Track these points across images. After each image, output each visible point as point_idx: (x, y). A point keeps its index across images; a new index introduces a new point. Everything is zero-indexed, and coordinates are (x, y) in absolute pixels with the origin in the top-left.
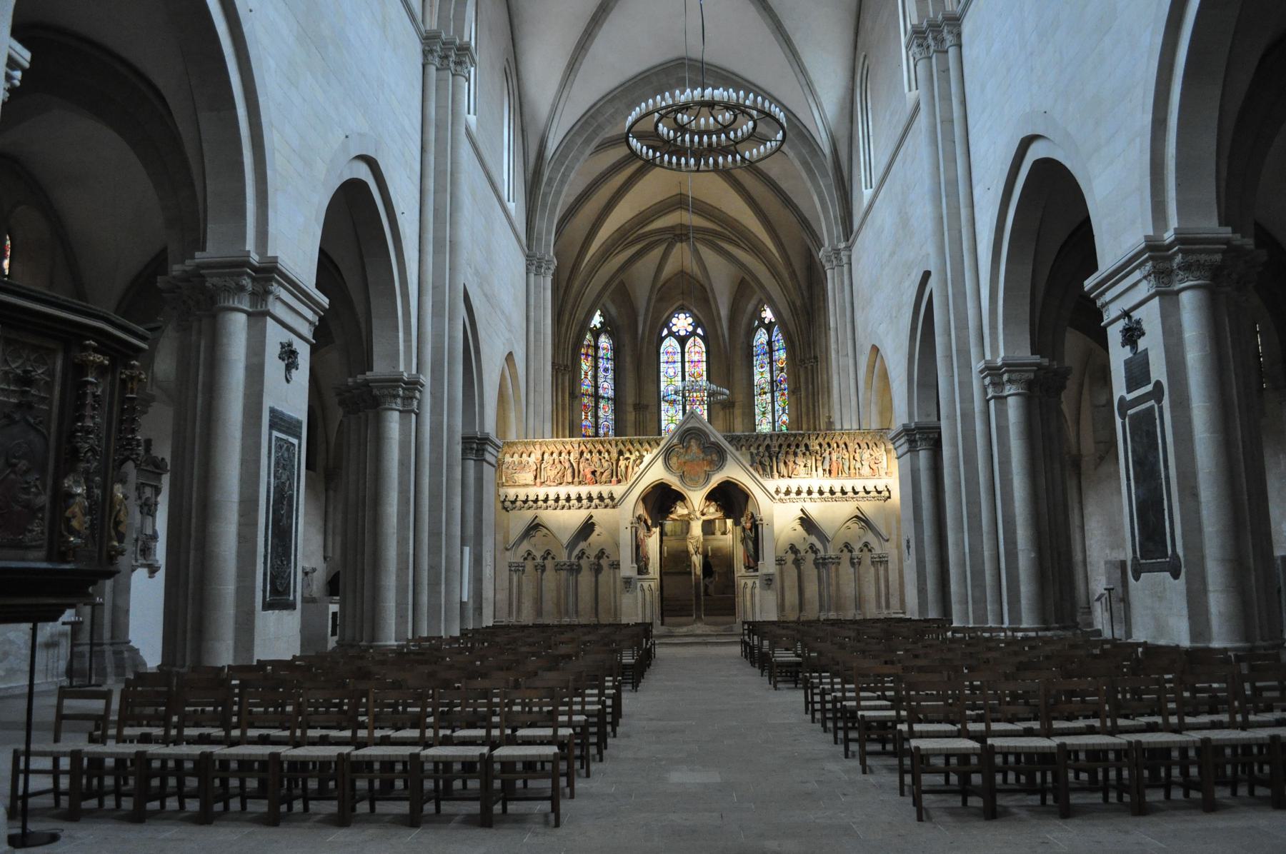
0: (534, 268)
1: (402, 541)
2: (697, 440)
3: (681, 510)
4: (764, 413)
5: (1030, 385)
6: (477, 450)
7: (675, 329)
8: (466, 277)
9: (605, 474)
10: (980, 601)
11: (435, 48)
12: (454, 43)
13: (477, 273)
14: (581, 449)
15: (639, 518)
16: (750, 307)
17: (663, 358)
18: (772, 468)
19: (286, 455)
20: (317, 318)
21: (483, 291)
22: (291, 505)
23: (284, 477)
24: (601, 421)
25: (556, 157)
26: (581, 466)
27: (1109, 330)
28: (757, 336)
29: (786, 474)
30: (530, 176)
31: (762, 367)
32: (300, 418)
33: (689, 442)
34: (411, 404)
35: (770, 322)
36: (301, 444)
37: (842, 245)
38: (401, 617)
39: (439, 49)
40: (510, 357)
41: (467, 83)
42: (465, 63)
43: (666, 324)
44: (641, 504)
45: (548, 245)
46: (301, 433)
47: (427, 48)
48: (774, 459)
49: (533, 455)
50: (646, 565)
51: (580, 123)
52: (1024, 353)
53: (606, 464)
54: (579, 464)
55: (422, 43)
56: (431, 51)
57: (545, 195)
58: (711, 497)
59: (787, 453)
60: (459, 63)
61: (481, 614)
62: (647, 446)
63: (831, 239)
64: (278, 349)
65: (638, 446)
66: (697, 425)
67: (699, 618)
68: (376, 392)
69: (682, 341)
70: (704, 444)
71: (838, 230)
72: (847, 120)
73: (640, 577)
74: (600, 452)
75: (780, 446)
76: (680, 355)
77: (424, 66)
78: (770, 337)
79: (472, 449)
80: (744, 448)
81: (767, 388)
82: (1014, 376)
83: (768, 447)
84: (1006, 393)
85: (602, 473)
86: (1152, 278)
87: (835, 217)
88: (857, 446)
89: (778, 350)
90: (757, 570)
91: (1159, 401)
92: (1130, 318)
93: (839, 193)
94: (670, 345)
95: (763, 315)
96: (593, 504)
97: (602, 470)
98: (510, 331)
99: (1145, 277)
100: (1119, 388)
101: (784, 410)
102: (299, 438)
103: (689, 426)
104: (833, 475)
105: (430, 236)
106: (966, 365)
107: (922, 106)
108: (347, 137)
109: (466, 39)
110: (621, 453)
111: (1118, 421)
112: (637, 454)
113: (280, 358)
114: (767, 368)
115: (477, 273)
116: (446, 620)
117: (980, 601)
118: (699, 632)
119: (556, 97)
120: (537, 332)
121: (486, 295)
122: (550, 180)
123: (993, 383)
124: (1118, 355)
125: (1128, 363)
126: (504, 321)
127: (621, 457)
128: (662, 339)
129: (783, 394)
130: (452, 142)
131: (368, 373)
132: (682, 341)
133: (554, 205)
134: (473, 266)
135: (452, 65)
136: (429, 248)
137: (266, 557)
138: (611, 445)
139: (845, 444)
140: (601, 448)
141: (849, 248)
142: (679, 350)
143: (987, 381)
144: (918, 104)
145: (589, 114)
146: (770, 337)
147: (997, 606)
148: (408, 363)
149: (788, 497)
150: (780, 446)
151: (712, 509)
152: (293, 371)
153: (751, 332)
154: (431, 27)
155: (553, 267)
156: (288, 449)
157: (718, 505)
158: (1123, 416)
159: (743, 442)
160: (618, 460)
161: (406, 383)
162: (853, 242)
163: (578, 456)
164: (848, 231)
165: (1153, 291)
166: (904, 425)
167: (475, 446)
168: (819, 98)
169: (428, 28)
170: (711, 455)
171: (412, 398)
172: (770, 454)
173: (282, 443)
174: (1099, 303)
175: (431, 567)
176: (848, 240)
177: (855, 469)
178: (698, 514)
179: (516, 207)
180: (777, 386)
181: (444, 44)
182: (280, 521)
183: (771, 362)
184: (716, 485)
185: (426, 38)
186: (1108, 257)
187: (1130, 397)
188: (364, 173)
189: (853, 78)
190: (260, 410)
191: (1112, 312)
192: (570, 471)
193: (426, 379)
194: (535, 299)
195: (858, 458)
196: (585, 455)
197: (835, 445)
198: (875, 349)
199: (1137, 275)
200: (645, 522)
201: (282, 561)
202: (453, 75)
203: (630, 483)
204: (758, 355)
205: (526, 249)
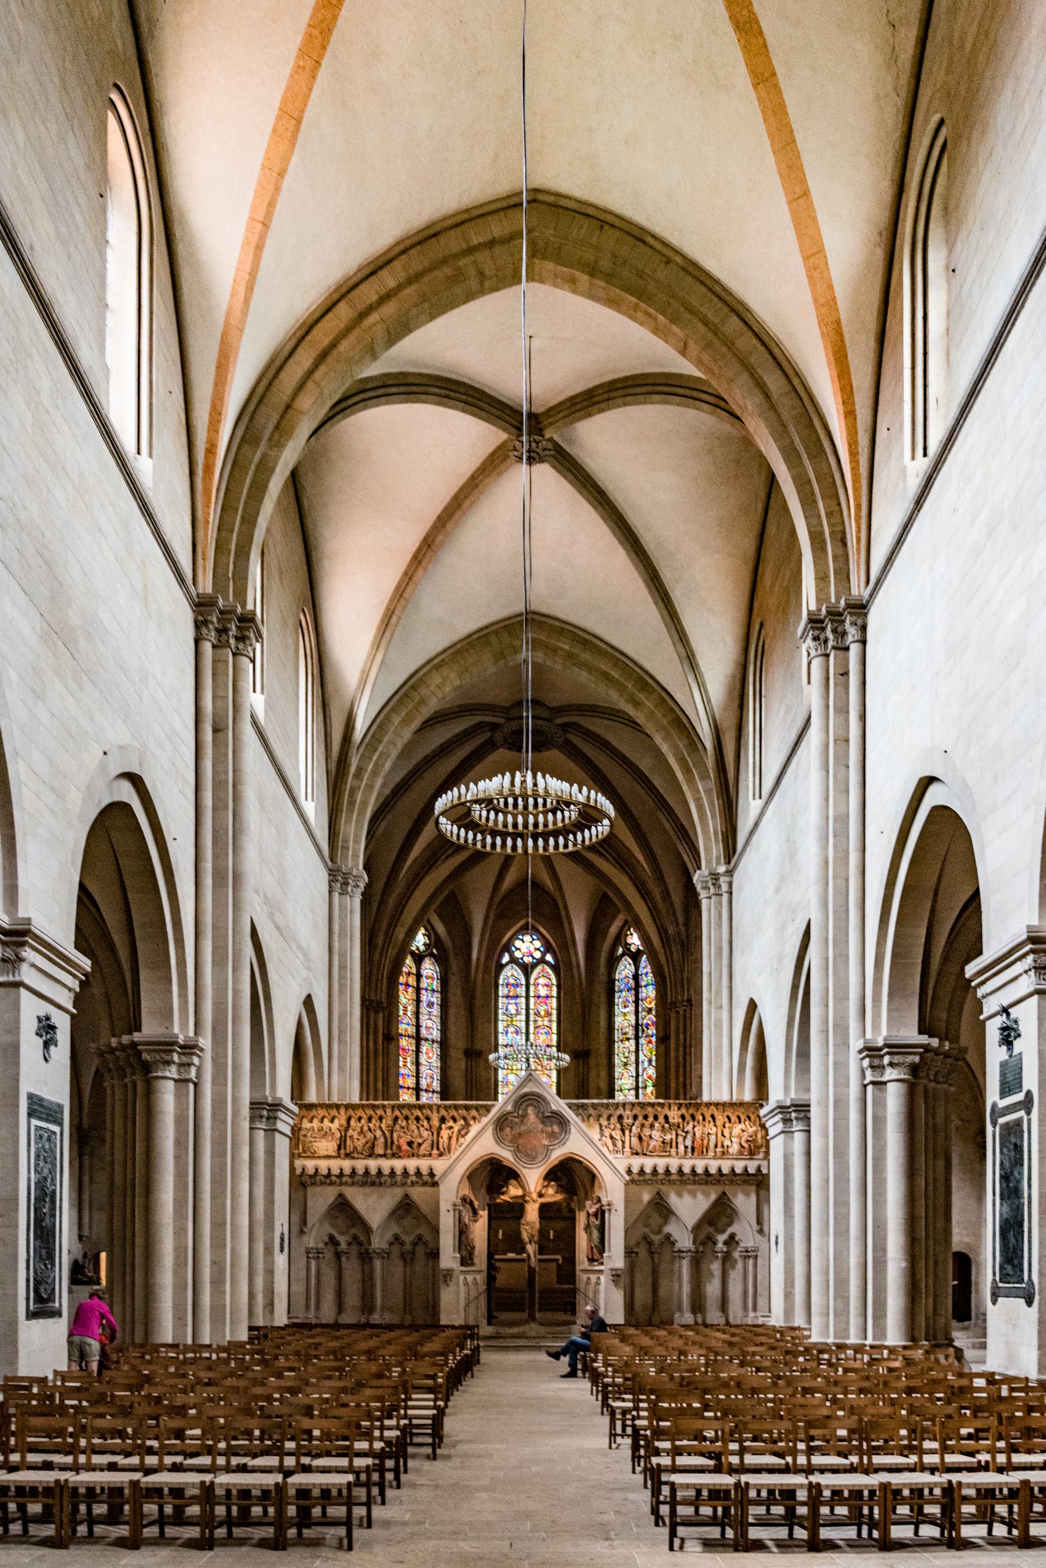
0: (339, 885)
1: (179, 1232)
2: (535, 1107)
3: (514, 1191)
4: (626, 1064)
5: (914, 1070)
6: (268, 1118)
7: (518, 954)
8: (255, 907)
9: (424, 1146)
10: (842, 1314)
11: (209, 618)
12: (234, 612)
13: (266, 900)
15: (464, 1199)
16: (614, 929)
17: (502, 991)
18: (623, 1142)
19: (47, 1146)
20: (77, 983)
21: (274, 922)
22: (53, 1202)
23: (46, 1171)
24: (422, 1069)
25: (366, 741)
26: (395, 1135)
27: (988, 1023)
28: (621, 967)
29: (639, 1150)
30: (333, 766)
31: (625, 1007)
32: (61, 1102)
33: (526, 1110)
34: (189, 1072)
35: (638, 950)
36: (63, 1134)
37: (722, 869)
38: (179, 1319)
39: (215, 620)
40: (308, 1003)
41: (251, 665)
42: (249, 638)
43: (507, 948)
44: (466, 1183)
45: (356, 856)
46: (62, 1119)
47: (200, 618)
48: (627, 1132)
49: (336, 1121)
50: (471, 1254)
51: (397, 697)
52: (910, 1034)
53: (425, 1134)
54: (392, 1133)
55: (194, 611)
56: (206, 623)
57: (353, 791)
58: (551, 1176)
59: (643, 1125)
60: (241, 639)
61: (272, 1312)
62: (474, 1113)
63: (708, 861)
64: (35, 1025)
66: (536, 1090)
67: (532, 1318)
68: (145, 1056)
69: (527, 970)
71: (717, 849)
72: (735, 705)
73: (463, 1268)
74: (417, 1119)
75: (635, 1117)
76: (524, 988)
77: (197, 642)
78: (637, 968)
79: (261, 1117)
80: (591, 1119)
81: (631, 1033)
82: (896, 1059)
84: (885, 1079)
85: (420, 1145)
86: (1032, 973)
87: (715, 833)
88: (726, 1119)
89: (646, 986)
91: (1029, 1113)
92: (1008, 1014)
93: (721, 802)
94: (511, 973)
95: (629, 940)
96: (409, 1181)
98: (308, 968)
99: (1026, 972)
100: (992, 1095)
101: (650, 1061)
102: (61, 1124)
103: (526, 1090)
104: (696, 1154)
105: (208, 865)
106: (843, 1043)
107: (814, 720)
108: (105, 753)
109: (250, 606)
110: (443, 1120)
111: (989, 1128)
112: (462, 1122)
113: (37, 1034)
114: (631, 1008)
115: (266, 900)
116: (232, 1322)
117: (842, 1314)
118: (532, 1333)
119: (366, 662)
120: (342, 967)
121: (278, 928)
122: (360, 771)
123: (872, 1067)
124: (995, 1055)
125: (1003, 1065)
126: (300, 955)
127: (443, 1126)
128: (501, 967)
129: (650, 1042)
130: (234, 745)
131: (135, 1034)
132: (527, 970)
133: (364, 803)
134: (261, 895)
135: (232, 641)
136: (208, 881)
137: (28, 1261)
139: (713, 1117)
140: (420, 1114)
141: (730, 873)
142: (523, 982)
143: (866, 1062)
144: (810, 717)
145: (410, 684)
146: (637, 968)
147: (861, 1321)
148: (184, 1024)
150: (635, 1117)
151: (551, 1191)
152: (52, 1048)
153: (613, 962)
154: (204, 588)
155: (362, 885)
156: (49, 1140)
157: (559, 1186)
158: (994, 1124)
160: (440, 1128)
161: (182, 1047)
162: (735, 866)
163: (390, 1122)
164: (730, 851)
165: (1031, 989)
166: (778, 1101)
167: (265, 1113)
168: (700, 673)
169: (201, 591)
171: (189, 1065)
172: (622, 1126)
173: (41, 1132)
174: (979, 994)
175: (213, 1262)
176: (729, 863)
177: (723, 1146)
178: (534, 1196)
179: (315, 808)
180: (643, 1030)
181: (222, 612)
182: (42, 1220)
183: (636, 1002)
184: (556, 1162)
185: (198, 605)
186: (993, 946)
187: (1002, 1103)
188: (127, 793)
189: (746, 650)
190: (17, 1096)
191: (990, 1006)
192: (382, 1140)
193: (206, 1042)
194: (340, 925)
195: (726, 1132)
196: (400, 1122)
197: (701, 1118)
198: (752, 1006)
199: (1018, 968)
200: (471, 1204)
201: (45, 1265)
202: (234, 654)
203: (452, 1160)
204: (621, 991)
205: (328, 861)
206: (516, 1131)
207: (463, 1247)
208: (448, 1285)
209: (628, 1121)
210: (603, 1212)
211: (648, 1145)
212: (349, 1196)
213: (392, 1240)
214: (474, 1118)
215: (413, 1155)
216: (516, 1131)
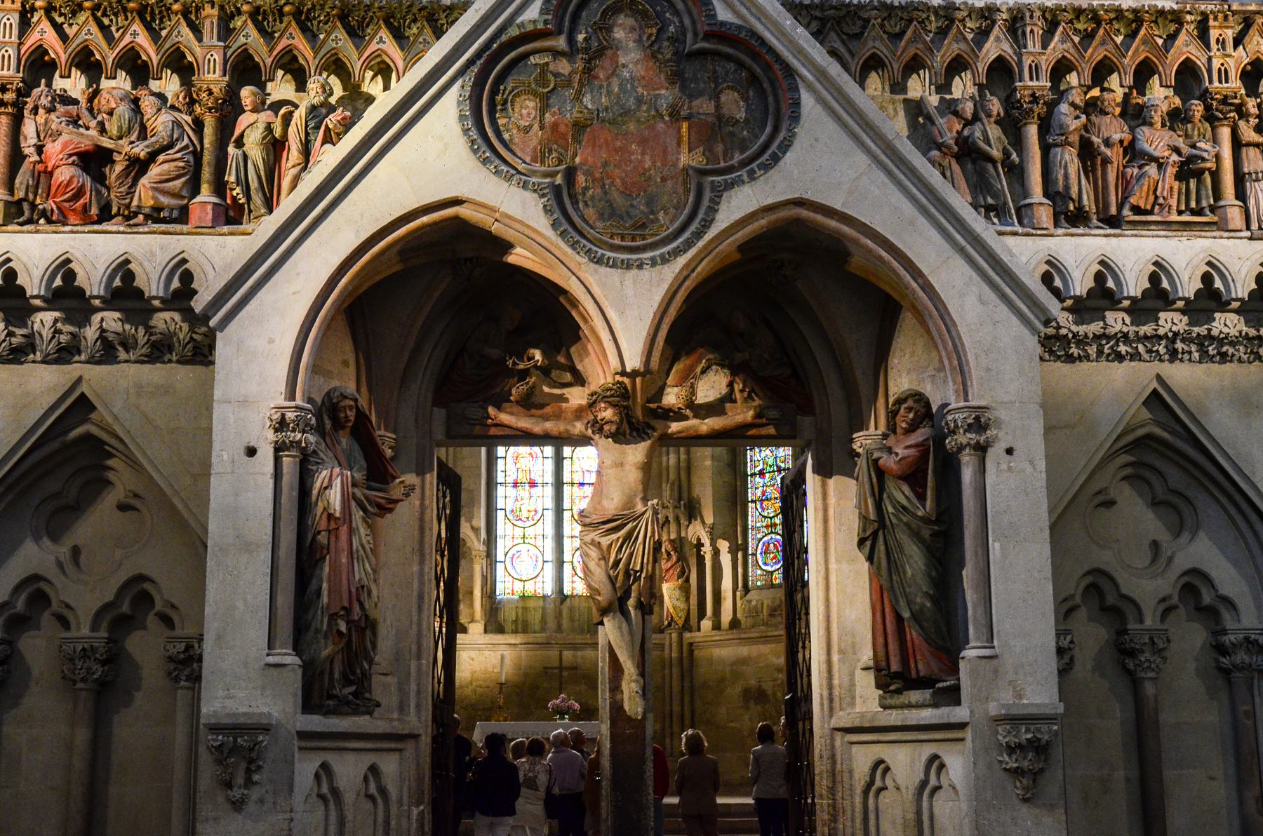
9: (155, 171)
14: (32, 39)
18: (1017, 173)
26: (29, 128)
29: (1088, 202)
33: (604, 27)
48: (1032, 131)
59: (1092, 107)
65: (339, 40)
70: (677, 40)
73: (315, 722)
83: (1002, 71)
85: (139, 167)
90: (952, 696)
97: (141, 150)
138: (196, 31)
140: (143, 40)
149: (1095, 328)
159: (875, 44)
170: (716, 96)
200: (362, 431)
210: (949, 467)
211: (1126, 185)
214: (384, 71)
215: (105, 215)
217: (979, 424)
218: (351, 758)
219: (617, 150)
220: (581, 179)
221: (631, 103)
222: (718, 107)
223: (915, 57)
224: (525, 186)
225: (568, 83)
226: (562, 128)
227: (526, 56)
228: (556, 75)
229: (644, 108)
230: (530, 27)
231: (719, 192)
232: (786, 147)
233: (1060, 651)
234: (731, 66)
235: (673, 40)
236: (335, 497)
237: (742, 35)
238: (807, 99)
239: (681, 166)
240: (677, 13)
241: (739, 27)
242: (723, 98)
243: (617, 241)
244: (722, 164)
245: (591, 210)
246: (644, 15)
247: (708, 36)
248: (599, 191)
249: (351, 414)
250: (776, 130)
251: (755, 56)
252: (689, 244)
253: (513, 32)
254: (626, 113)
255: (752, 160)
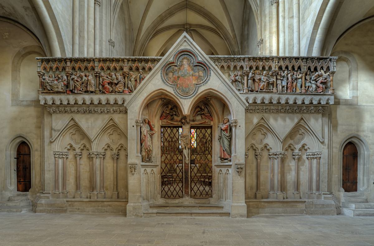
73: (144, 164)
90: (230, 161)
170: (199, 72)
206: (176, 75)
207: (143, 150)
208: (133, 174)
209: (246, 69)
212: (77, 120)
213: (106, 147)
216: (176, 75)
217: (236, 123)
218: (149, 168)
219: (184, 81)
220: (179, 86)
221: (186, 74)
222: (199, 74)
223: (229, 66)
224: (170, 87)
225: (176, 71)
226: (176, 78)
227: (171, 66)
228: (175, 69)
229: (188, 74)
230: (171, 62)
231: (199, 87)
232: (209, 80)
233: (246, 155)
234: (201, 67)
235: (192, 63)
236: (145, 133)
237: (203, 62)
238: (212, 72)
239: (193, 83)
240: (193, 59)
241: (202, 61)
242: (200, 72)
243: (184, 95)
244: (199, 83)
245: (180, 90)
246: (188, 59)
247: (198, 63)
248: (181, 87)
249: (147, 121)
250: (207, 77)
251: (205, 66)
252: (194, 95)
253: (169, 63)
254: (185, 75)
255: (204, 82)
